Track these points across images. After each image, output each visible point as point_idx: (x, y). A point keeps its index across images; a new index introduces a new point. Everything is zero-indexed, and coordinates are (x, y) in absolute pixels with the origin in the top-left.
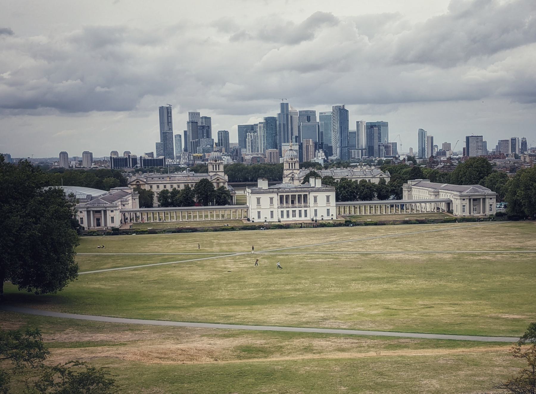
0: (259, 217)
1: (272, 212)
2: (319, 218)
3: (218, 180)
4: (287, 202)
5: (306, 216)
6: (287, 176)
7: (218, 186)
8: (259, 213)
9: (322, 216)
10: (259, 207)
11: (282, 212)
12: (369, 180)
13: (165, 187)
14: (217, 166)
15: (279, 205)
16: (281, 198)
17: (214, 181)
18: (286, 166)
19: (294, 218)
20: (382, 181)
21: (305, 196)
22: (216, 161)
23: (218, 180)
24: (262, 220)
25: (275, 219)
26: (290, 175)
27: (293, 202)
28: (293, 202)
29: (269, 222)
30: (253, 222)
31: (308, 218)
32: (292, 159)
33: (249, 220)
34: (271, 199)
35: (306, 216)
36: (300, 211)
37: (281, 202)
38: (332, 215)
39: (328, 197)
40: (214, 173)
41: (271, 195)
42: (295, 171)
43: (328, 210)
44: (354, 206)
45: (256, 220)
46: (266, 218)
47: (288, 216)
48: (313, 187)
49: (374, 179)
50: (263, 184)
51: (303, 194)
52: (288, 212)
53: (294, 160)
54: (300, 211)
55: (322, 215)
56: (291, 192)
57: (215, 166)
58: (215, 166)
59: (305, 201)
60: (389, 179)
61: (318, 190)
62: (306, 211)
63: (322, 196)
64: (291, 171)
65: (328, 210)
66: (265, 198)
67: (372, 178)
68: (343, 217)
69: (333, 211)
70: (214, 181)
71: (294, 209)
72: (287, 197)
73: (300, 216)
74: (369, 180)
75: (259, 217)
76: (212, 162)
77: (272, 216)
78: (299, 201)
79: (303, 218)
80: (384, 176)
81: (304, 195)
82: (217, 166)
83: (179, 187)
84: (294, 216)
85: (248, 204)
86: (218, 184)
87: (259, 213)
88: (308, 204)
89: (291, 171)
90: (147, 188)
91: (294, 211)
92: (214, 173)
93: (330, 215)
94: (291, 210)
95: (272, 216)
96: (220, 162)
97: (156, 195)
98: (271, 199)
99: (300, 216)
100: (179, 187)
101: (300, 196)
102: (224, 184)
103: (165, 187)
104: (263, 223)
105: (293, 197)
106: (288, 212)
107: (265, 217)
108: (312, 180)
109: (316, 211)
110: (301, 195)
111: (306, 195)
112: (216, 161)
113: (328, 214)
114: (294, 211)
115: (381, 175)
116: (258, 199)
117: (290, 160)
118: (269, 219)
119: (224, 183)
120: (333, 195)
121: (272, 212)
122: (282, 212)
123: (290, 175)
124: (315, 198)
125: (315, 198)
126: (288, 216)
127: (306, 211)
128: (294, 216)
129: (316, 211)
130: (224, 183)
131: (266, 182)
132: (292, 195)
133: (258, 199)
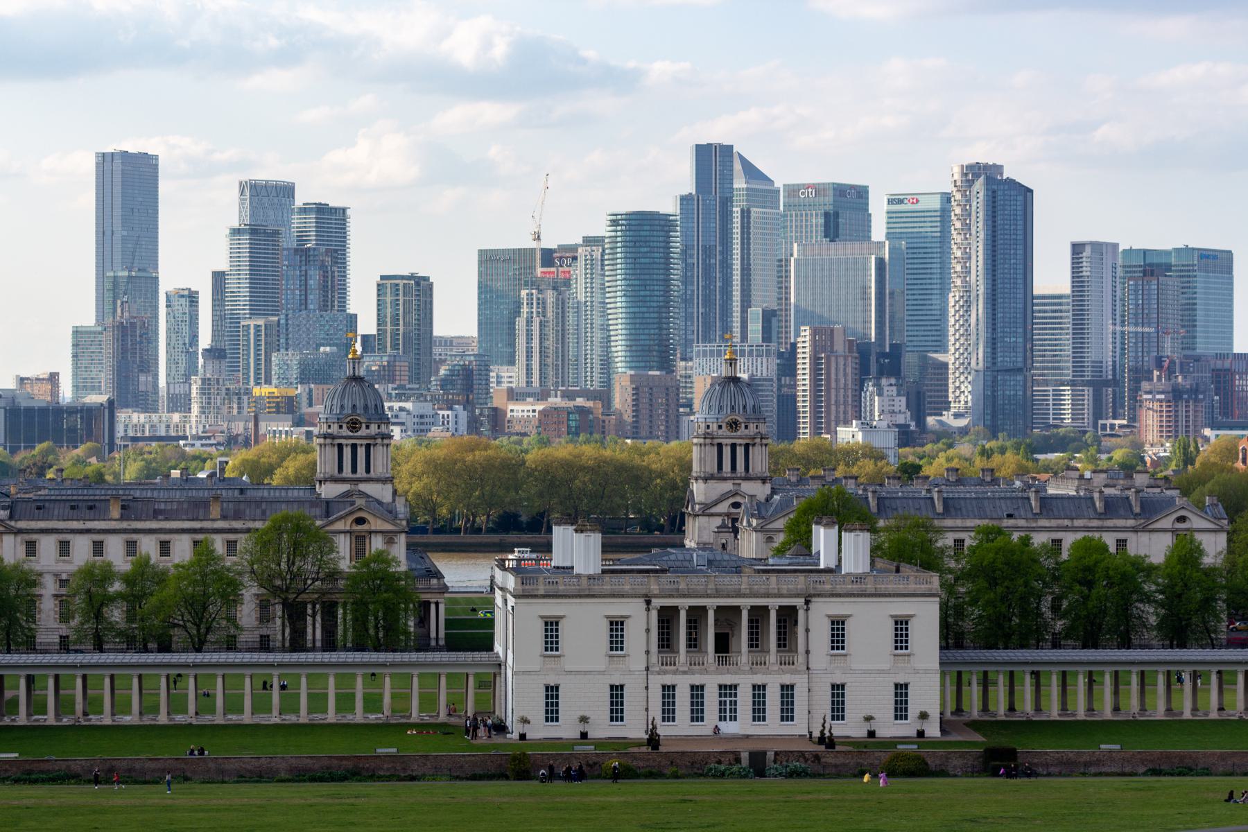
0: (552, 713)
1: (617, 692)
2: (850, 728)
3: (360, 521)
4: (693, 643)
5: (787, 714)
6: (706, 510)
8: (552, 692)
9: (869, 719)
10: (551, 664)
11: (669, 690)
12: (1121, 544)
13: (98, 548)
14: (361, 452)
15: (654, 658)
16: (667, 618)
17: (340, 526)
19: (728, 728)
20: (1187, 554)
21: (788, 617)
22: (354, 426)
23: (360, 521)
24: (566, 729)
25: (633, 728)
26: (724, 507)
27: (723, 645)
28: (723, 645)
29: (599, 743)
30: (523, 737)
31: (798, 727)
32: (733, 425)
33: (501, 728)
34: (617, 626)
35: (787, 714)
36: (759, 691)
37: (666, 641)
38: (924, 716)
39: (901, 627)
40: (345, 487)
41: (617, 608)
42: (747, 487)
43: (901, 690)
44: (1036, 675)
45: (539, 730)
46: (584, 720)
47: (697, 714)
48: (828, 571)
49: (1144, 537)
50: (575, 548)
51: (774, 603)
52: (697, 691)
53: (742, 431)
54: (759, 691)
55: (869, 712)
56: (718, 595)
57: (347, 452)
58: (347, 452)
60: (1223, 538)
62: (787, 691)
63: (870, 622)
64: (728, 486)
65: (901, 690)
66: (585, 623)
67: (1135, 530)
68: (975, 725)
69: (928, 696)
70: (340, 526)
71: (728, 680)
72: (697, 615)
73: (759, 713)
74: (1121, 544)
75: (552, 713)
76: (334, 429)
77: (617, 713)
78: (755, 641)
79: (772, 726)
80: (1196, 522)
81: (781, 610)
82: (361, 452)
83: (165, 549)
84: (728, 712)
85: (498, 648)
86: (360, 541)
87: (552, 692)
88: (801, 658)
89: (728, 486)
91: (728, 691)
92: (345, 487)
93: (913, 711)
94: (712, 684)
95: (617, 713)
96: (374, 429)
97: (49, 588)
98: (617, 626)
99: (759, 713)
100: (165, 549)
101: (759, 615)
102: (390, 542)
103: (98, 548)
104: (571, 743)
105: (728, 615)
106: (697, 691)
108: (823, 537)
109: (838, 691)
110: (765, 609)
111: (793, 610)
113: (901, 711)
114: (728, 691)
115: (1182, 519)
116: (552, 628)
117: (725, 431)
118: (603, 729)
119: (390, 537)
120: (926, 618)
121: (617, 692)
122: (669, 690)
123: (724, 507)
124: (838, 628)
125: (838, 628)
126: (697, 714)
127: (787, 691)
128: (728, 712)
129: (838, 691)
130: (390, 537)
131: (595, 539)
132: (719, 610)
133: (552, 628)
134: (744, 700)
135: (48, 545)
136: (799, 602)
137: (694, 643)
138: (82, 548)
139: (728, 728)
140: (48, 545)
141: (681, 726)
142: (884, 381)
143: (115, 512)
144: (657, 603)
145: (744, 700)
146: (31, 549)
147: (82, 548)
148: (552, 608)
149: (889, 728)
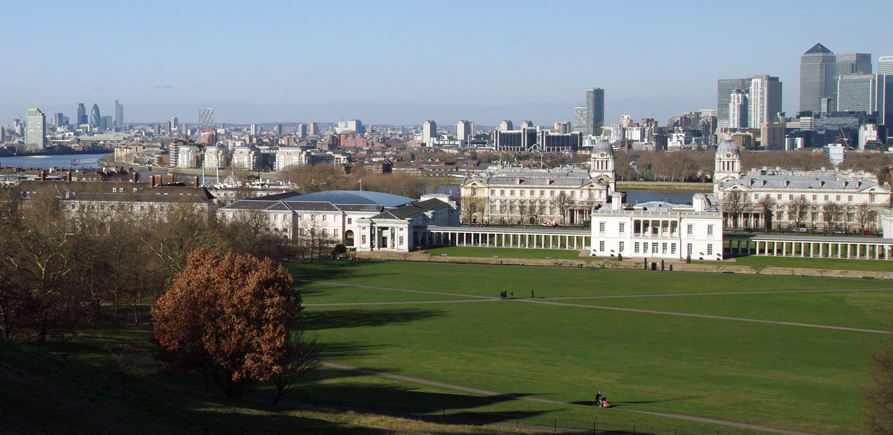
0: (602, 249)
2: (695, 256)
7: (591, 195)
8: (602, 244)
11: (637, 244)
12: (850, 198)
13: (512, 193)
16: (637, 225)
18: (718, 166)
19: (655, 255)
21: (674, 224)
24: (607, 253)
27: (655, 231)
28: (655, 231)
31: (676, 256)
32: (728, 156)
34: (622, 226)
39: (710, 228)
43: (710, 247)
45: (599, 254)
51: (670, 220)
52: (645, 244)
59: (672, 231)
60: (889, 196)
61: (697, 215)
62: (673, 245)
63: (700, 226)
65: (710, 247)
66: (612, 223)
69: (718, 249)
71: (655, 241)
72: (646, 224)
74: (850, 198)
75: (602, 249)
76: (596, 156)
79: (668, 255)
82: (604, 163)
89: (725, 175)
90: (483, 193)
95: (621, 248)
98: (622, 226)
100: (532, 193)
103: (512, 193)
105: (655, 224)
106: (645, 244)
107: (611, 249)
109: (690, 246)
112: (602, 155)
113: (710, 252)
116: (602, 225)
122: (637, 244)
124: (690, 227)
125: (690, 227)
127: (673, 245)
129: (690, 246)
132: (653, 221)
133: (602, 225)
134: (660, 247)
135: (498, 191)
136: (678, 220)
137: (645, 231)
138: (507, 192)
139: (655, 255)
140: (498, 191)
141: (641, 254)
142: (868, 126)
143: (518, 182)
144: (634, 219)
145: (660, 247)
146: (493, 192)
147: (507, 192)
148: (602, 219)
149: (706, 257)
